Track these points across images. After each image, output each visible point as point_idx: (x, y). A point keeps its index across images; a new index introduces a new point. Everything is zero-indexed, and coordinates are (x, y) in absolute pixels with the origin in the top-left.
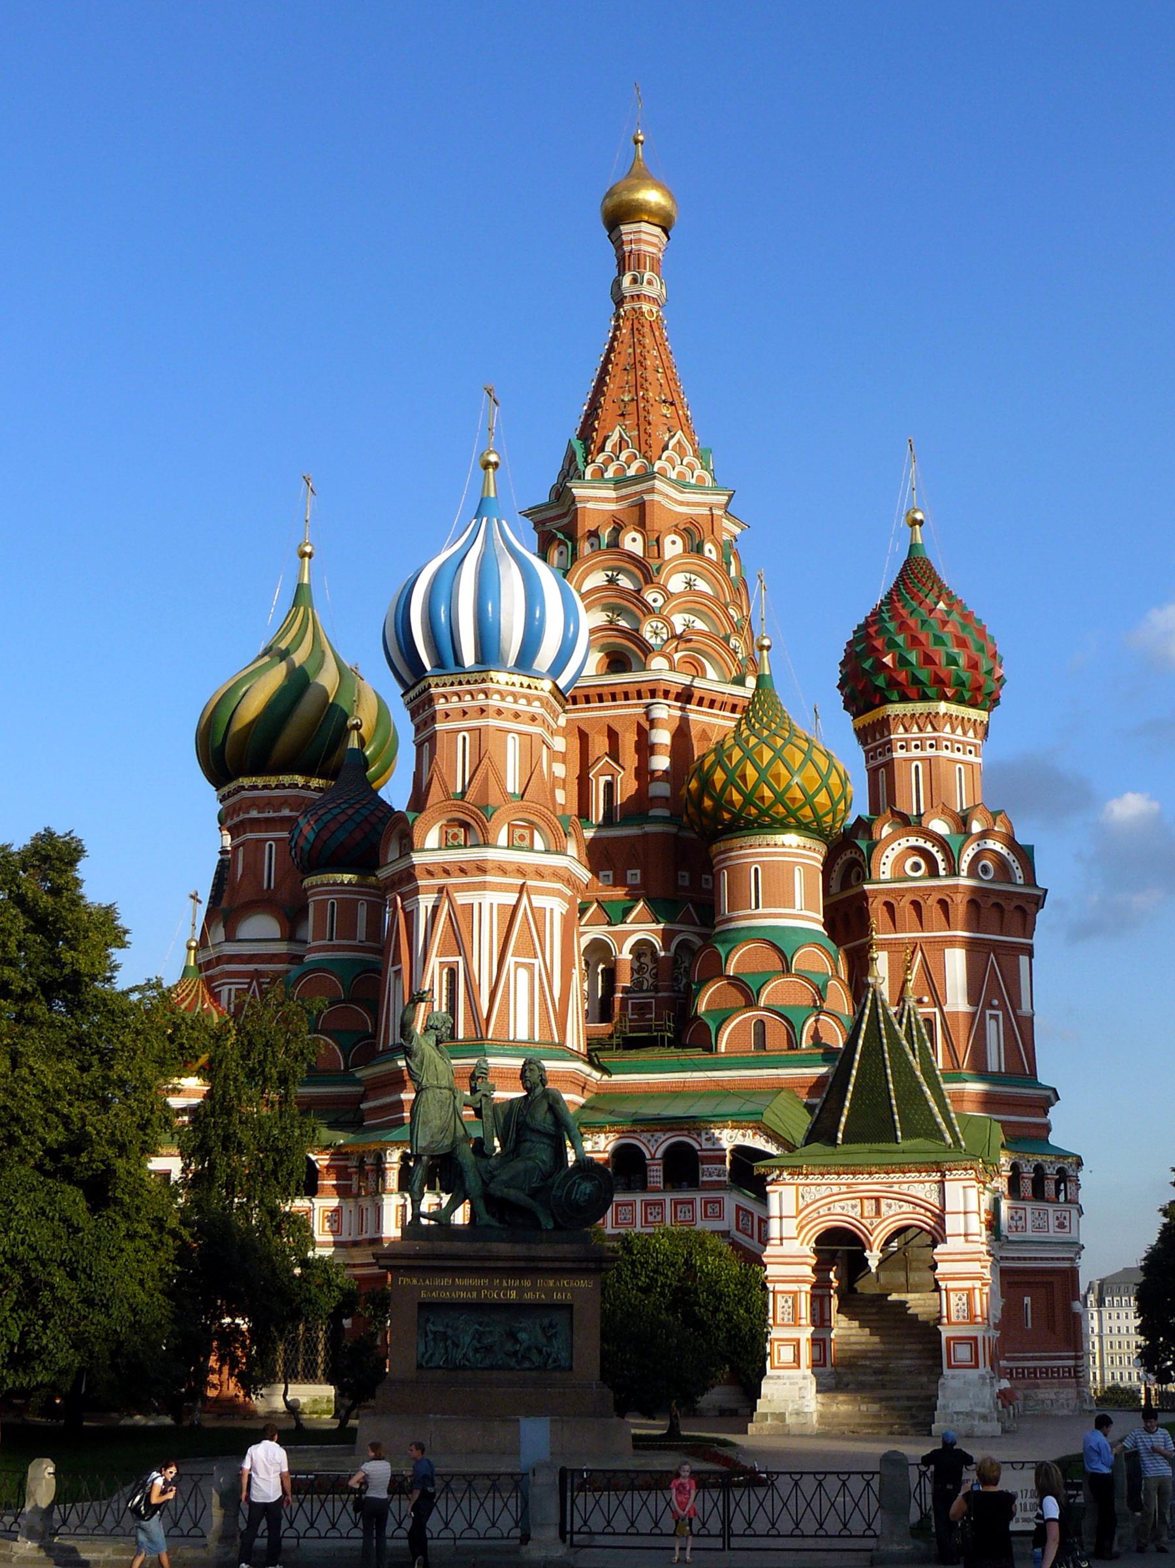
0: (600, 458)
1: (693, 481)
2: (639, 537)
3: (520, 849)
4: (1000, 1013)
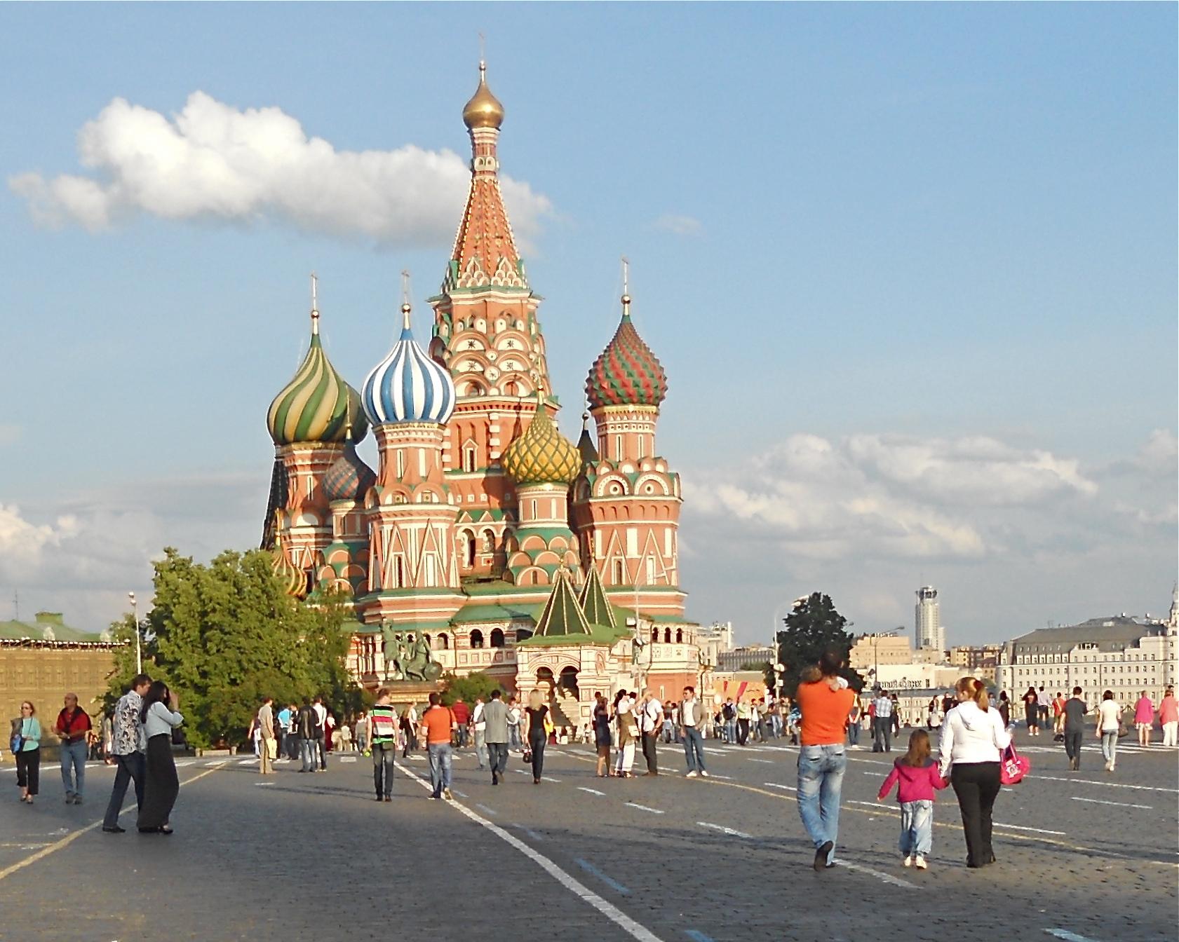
0: (464, 276)
1: (512, 285)
2: (484, 322)
3: (427, 503)
4: (654, 557)
